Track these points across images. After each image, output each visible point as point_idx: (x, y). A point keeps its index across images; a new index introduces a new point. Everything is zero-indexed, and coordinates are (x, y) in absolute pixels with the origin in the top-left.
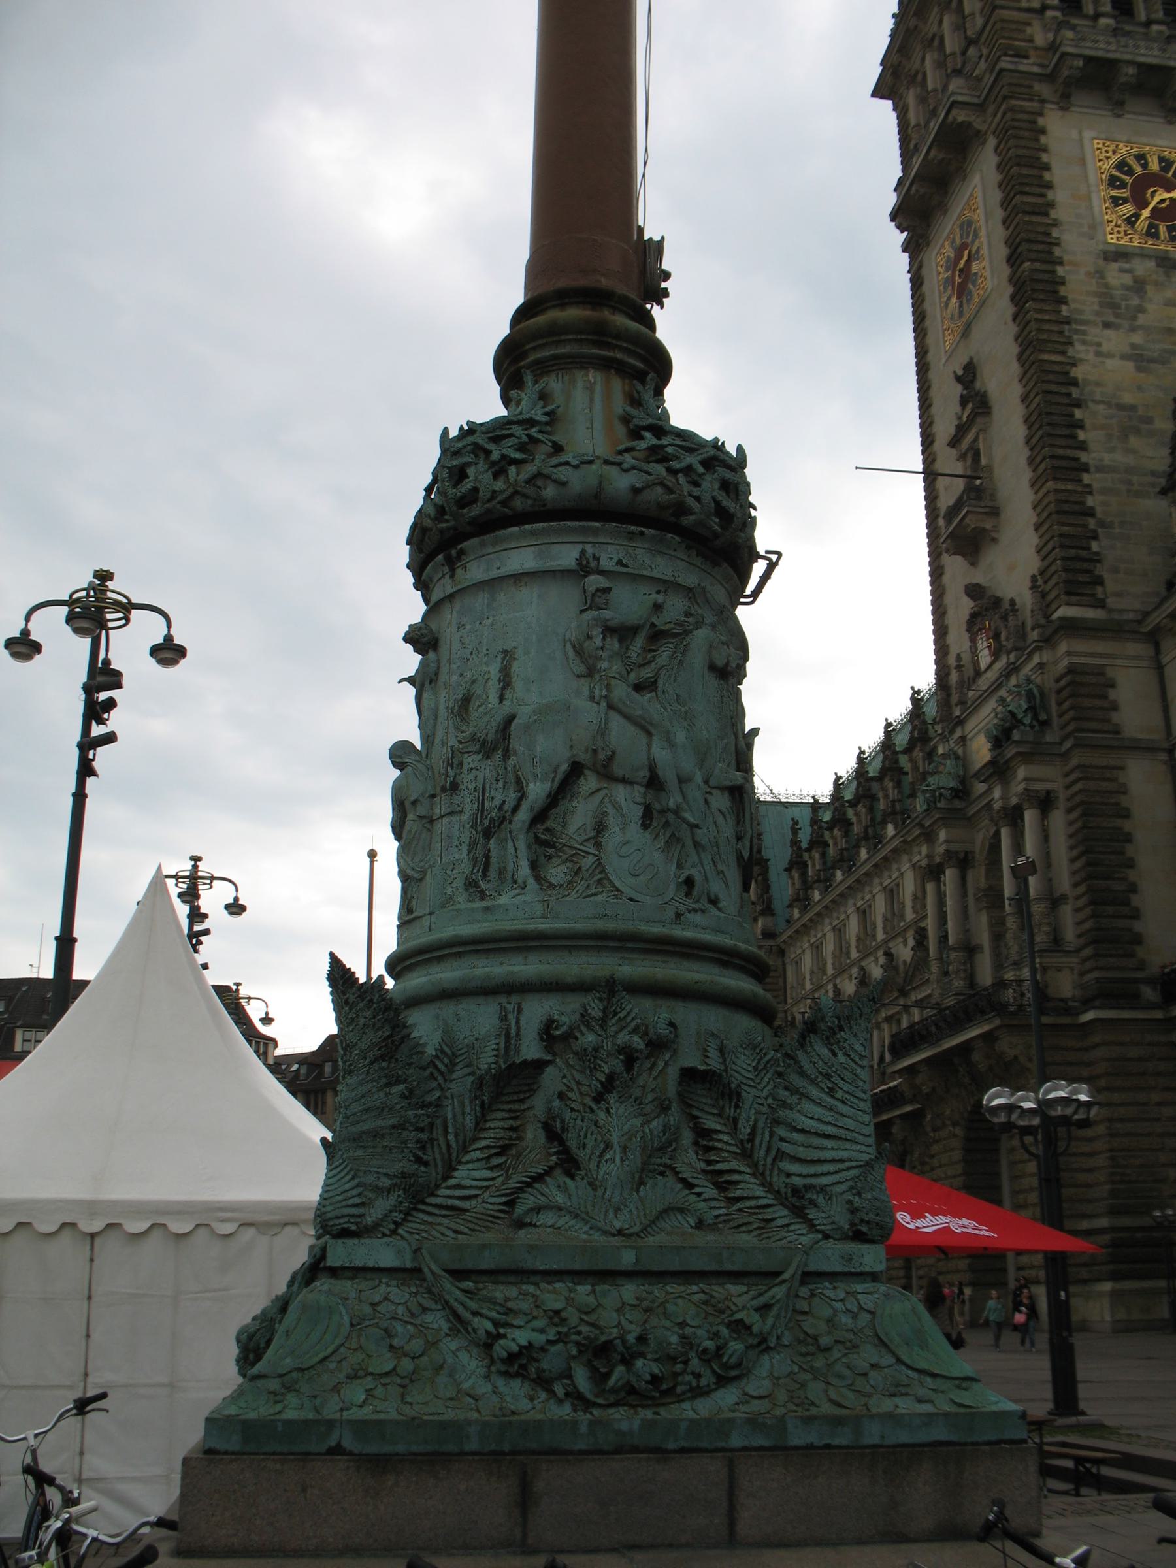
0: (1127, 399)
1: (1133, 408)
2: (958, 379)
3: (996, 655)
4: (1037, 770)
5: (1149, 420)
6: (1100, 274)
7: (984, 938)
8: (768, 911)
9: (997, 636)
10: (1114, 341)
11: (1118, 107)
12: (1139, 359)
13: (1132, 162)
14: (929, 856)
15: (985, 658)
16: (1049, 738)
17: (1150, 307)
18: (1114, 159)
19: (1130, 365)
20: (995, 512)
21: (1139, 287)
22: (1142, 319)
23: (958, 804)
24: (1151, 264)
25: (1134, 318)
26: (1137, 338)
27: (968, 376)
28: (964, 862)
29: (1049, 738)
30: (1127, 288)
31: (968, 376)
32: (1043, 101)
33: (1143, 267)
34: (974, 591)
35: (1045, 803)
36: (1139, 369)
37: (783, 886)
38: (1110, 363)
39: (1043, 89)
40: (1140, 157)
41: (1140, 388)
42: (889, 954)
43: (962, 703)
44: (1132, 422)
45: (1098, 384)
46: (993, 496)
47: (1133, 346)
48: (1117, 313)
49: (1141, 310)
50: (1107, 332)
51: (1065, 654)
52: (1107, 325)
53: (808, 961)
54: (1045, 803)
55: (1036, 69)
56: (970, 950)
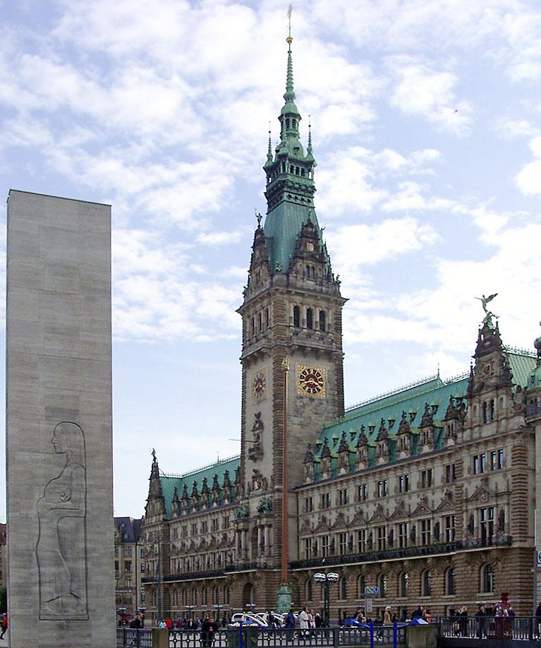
0: (297, 435)
1: (298, 438)
2: (256, 415)
3: (259, 487)
4: (269, 520)
5: (302, 441)
6: (295, 402)
7: (250, 548)
8: (165, 513)
9: (260, 483)
10: (296, 420)
11: (305, 355)
12: (302, 425)
13: (307, 371)
14: (237, 527)
15: (256, 487)
16: (272, 513)
17: (306, 412)
18: (303, 370)
19: (299, 427)
20: (262, 454)
21: (304, 406)
22: (304, 414)
23: (246, 518)
24: (308, 400)
25: (302, 414)
26: (302, 420)
27: (258, 416)
28: (246, 531)
29: (272, 513)
30: (301, 406)
31: (258, 416)
32: (287, 354)
33: (305, 400)
34: (255, 471)
35: (270, 526)
36: (301, 428)
37: (170, 507)
38: (295, 426)
39: (286, 349)
40: (308, 370)
41: (301, 433)
42: (213, 537)
43: (249, 494)
44: (299, 440)
45: (291, 431)
46: (262, 450)
47: (301, 422)
48: (298, 412)
49: (304, 412)
50: (296, 418)
51: (276, 495)
52: (295, 416)
53: (180, 530)
54: (270, 526)
55: (286, 345)
56: (247, 550)
